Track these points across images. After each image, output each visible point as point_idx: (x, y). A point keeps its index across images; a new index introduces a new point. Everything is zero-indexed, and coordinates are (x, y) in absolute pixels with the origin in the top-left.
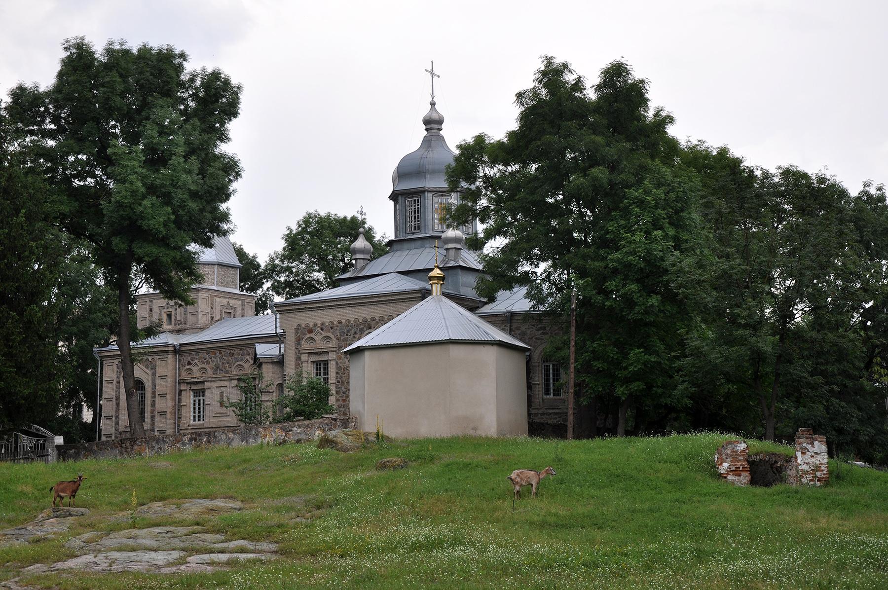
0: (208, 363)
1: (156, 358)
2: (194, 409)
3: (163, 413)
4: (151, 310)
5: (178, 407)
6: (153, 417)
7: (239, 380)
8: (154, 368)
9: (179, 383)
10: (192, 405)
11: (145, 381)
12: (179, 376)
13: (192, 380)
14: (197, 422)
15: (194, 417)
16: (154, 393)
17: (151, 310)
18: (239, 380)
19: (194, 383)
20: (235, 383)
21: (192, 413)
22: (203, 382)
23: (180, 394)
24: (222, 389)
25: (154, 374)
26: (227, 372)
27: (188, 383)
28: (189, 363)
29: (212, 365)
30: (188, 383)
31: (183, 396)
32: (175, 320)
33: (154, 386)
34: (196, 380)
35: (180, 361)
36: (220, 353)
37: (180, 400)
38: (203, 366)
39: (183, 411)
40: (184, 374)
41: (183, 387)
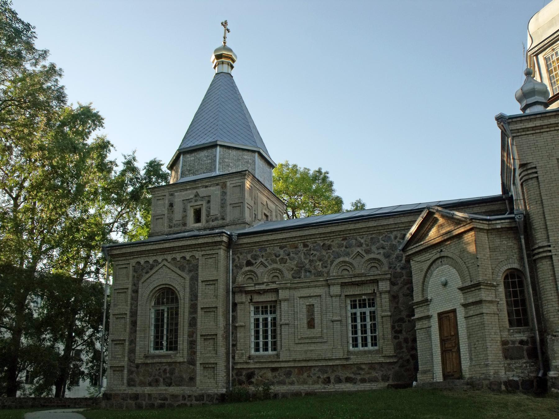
0: (283, 261)
1: (198, 254)
2: (257, 332)
3: (210, 337)
4: (171, 205)
5: (232, 328)
6: (192, 344)
7: (343, 285)
8: (194, 270)
9: (234, 293)
10: (252, 326)
11: (178, 288)
12: (234, 282)
13: (257, 287)
14: (261, 352)
15: (257, 344)
16: (193, 308)
17: (171, 205)
18: (343, 285)
19: (259, 292)
20: (336, 290)
21: (253, 339)
22: (276, 291)
23: (234, 310)
24: (312, 301)
25: (194, 279)
26: (320, 274)
27: (247, 292)
28: (249, 264)
29: (292, 264)
30: (247, 292)
31: (239, 312)
32: (208, 215)
33: (194, 296)
34: (263, 287)
35: (234, 260)
36: (305, 246)
37: (234, 318)
38: (275, 266)
39: (240, 334)
40: (240, 279)
41: (239, 298)
